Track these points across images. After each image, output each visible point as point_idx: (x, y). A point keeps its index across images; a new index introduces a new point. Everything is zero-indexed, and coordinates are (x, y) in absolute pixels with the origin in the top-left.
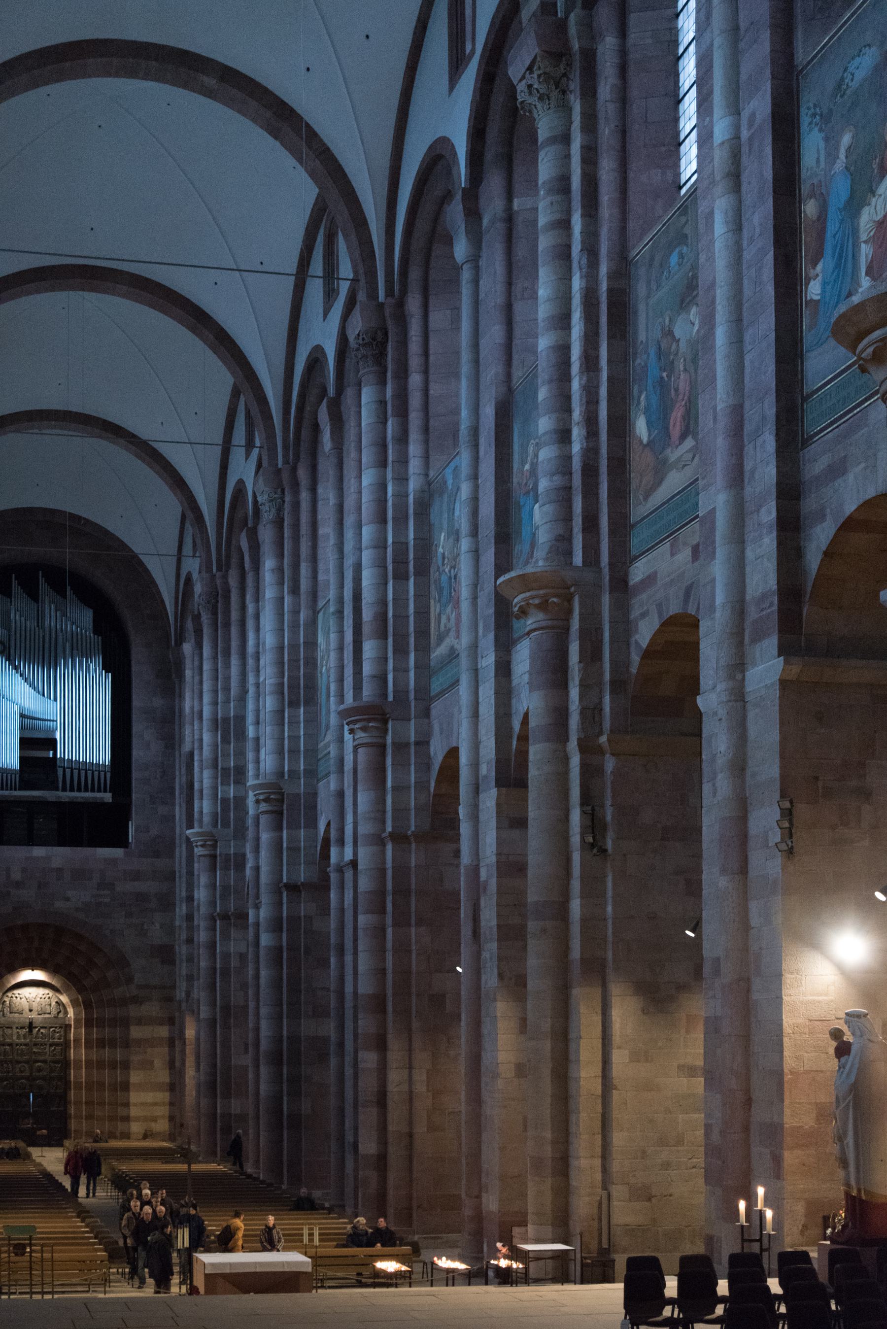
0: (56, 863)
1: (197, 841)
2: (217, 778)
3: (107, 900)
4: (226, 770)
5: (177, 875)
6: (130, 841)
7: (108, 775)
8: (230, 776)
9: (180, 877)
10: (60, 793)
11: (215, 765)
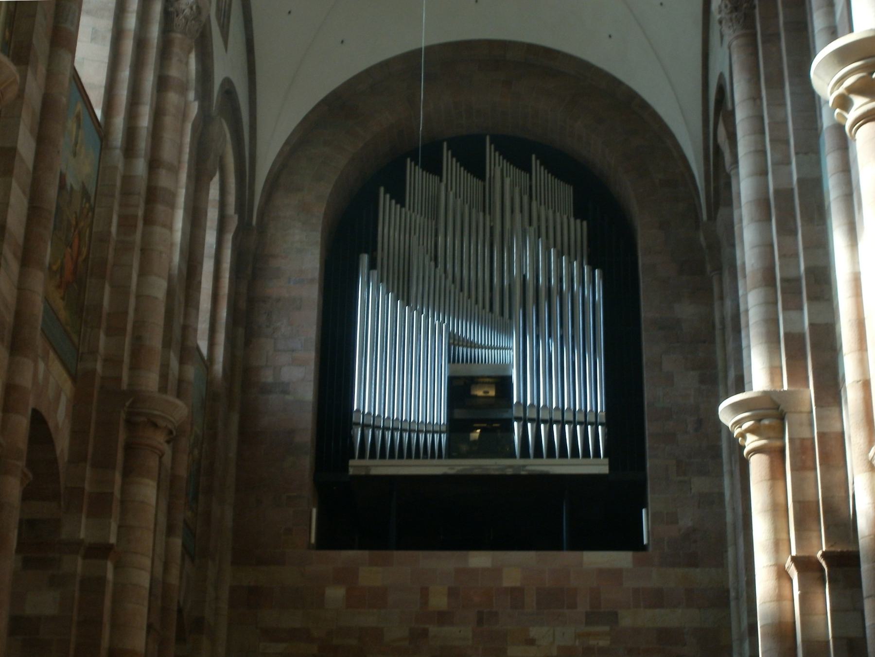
0: (511, 579)
1: (739, 423)
2: (776, 303)
3: (603, 643)
4: (791, 286)
5: (733, 594)
6: (645, 542)
8: (800, 293)
9: (737, 598)
10: (518, 461)
11: (768, 278)
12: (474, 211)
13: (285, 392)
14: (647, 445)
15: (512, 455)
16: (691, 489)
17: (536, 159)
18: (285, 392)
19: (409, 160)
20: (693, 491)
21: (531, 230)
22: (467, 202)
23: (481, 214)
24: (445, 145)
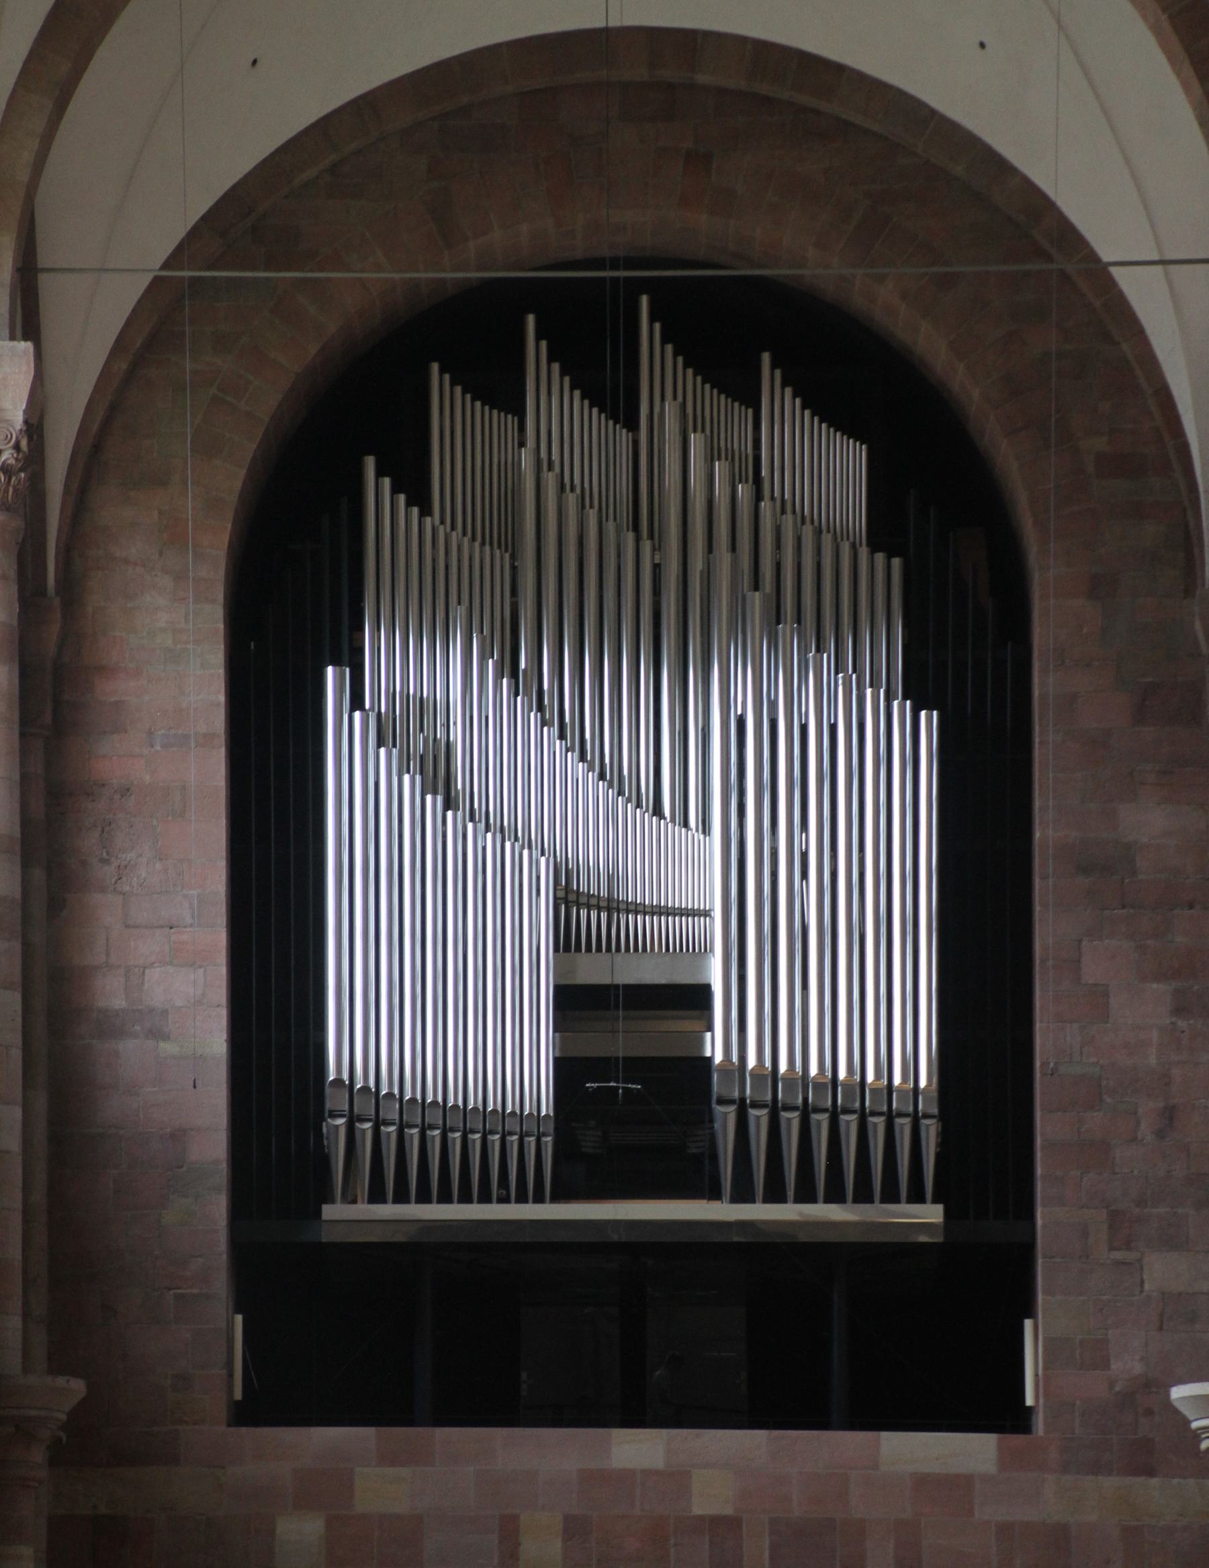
7: (931, 1132)
12: (610, 526)
13: (158, 1034)
14: (1039, 1171)
15: (714, 1194)
16: (1142, 1282)
17: (774, 366)
18: (158, 1034)
19: (435, 367)
20: (1147, 1287)
21: (756, 600)
22: (591, 507)
23: (631, 535)
24: (531, 319)
